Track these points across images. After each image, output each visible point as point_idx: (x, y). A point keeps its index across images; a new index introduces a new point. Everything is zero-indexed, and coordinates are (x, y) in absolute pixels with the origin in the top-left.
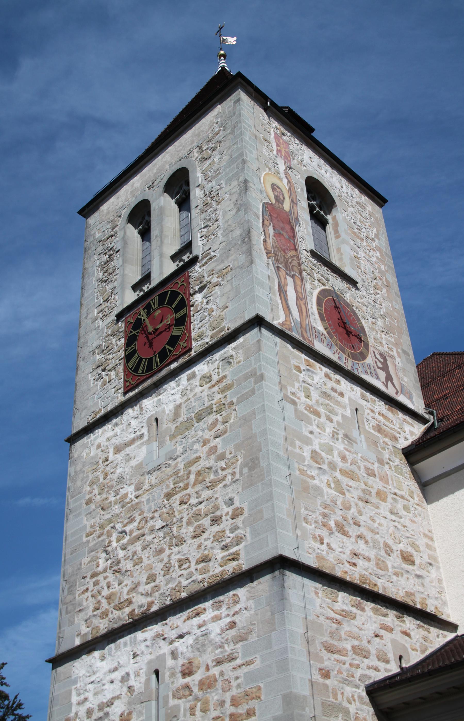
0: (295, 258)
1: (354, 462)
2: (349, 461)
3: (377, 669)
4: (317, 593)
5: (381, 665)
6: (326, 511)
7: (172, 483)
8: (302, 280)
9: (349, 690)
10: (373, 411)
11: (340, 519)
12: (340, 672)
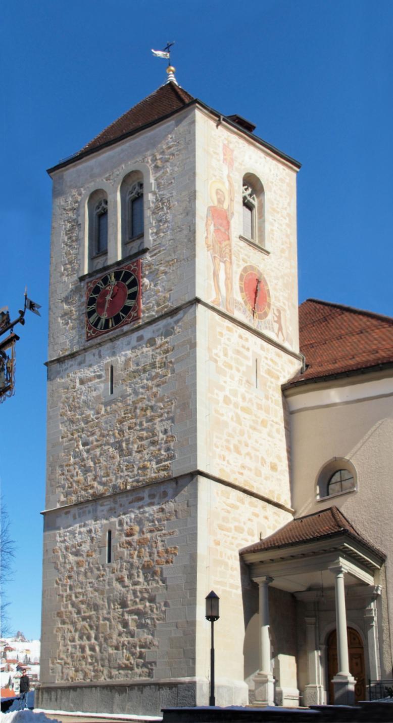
3: (247, 541)
5: (249, 538)
7: (123, 413)
8: (231, 263)
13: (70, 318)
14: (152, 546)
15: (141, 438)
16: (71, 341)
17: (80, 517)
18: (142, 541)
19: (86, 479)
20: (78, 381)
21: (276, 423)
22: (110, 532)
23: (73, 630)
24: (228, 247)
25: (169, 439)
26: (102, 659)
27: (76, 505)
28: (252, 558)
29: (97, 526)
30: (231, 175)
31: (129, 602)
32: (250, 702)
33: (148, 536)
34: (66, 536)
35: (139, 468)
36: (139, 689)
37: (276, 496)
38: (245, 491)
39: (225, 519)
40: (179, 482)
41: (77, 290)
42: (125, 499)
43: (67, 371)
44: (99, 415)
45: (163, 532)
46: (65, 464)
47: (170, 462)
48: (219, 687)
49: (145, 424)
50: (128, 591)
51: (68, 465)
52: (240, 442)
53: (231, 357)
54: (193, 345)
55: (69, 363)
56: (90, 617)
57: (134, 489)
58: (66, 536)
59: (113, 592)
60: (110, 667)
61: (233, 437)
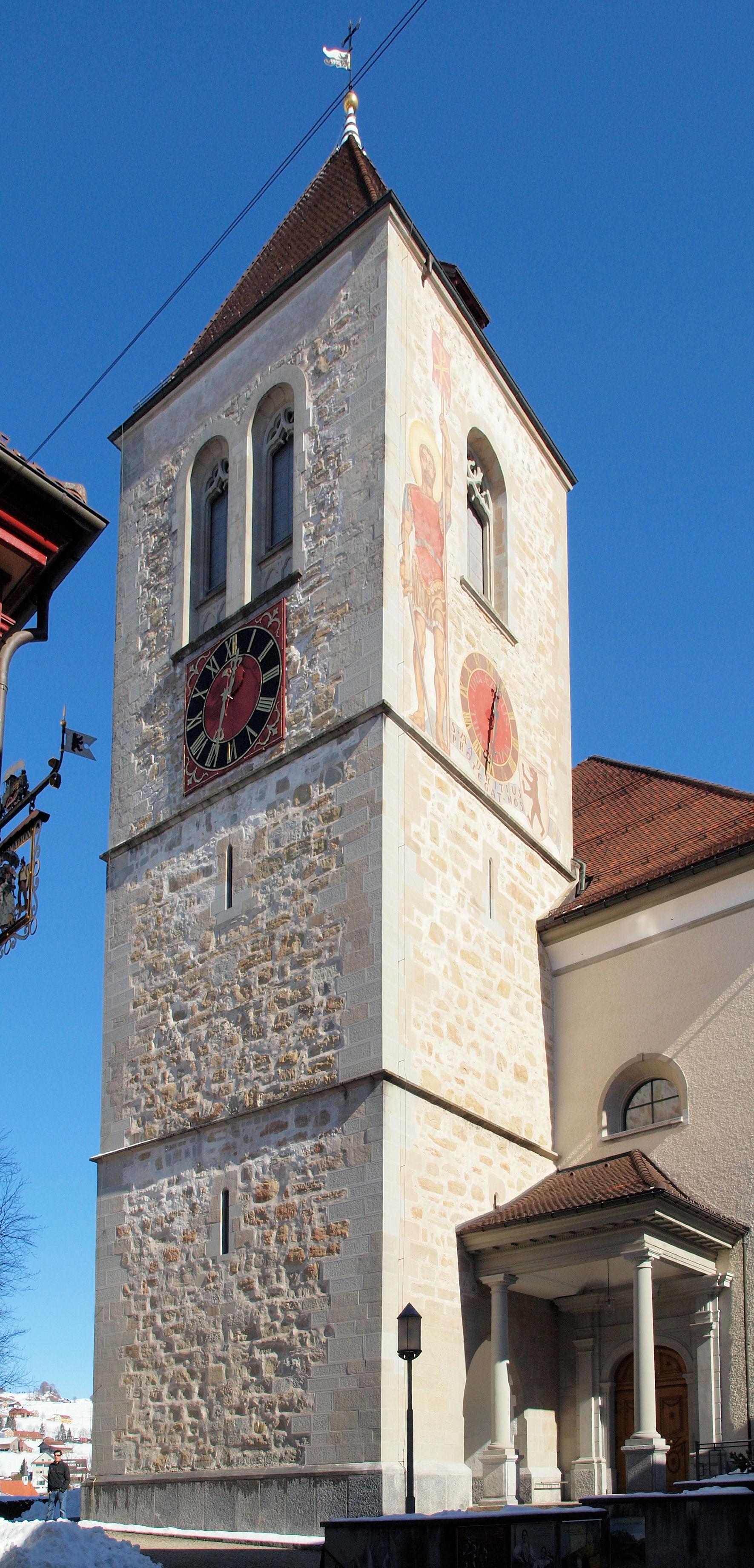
0: (439, 596)
1: (479, 940)
2: (473, 938)
4: (418, 1118)
5: (475, 1203)
6: (439, 1010)
9: (439, 1231)
10: (509, 862)
11: (453, 1021)
12: (433, 1211)
13: (154, 751)
14: (302, 1221)
15: (282, 1002)
16: (155, 800)
17: (169, 1163)
18: (284, 1210)
19: (180, 1087)
20: (166, 884)
21: (527, 992)
22: (226, 1194)
23: (157, 1380)
24: (439, 596)
25: (333, 1004)
26: (213, 1431)
27: (161, 1140)
28: (480, 1241)
29: (202, 1181)
30: (446, 418)
31: (262, 1329)
32: (476, 1500)
33: (296, 1199)
34: (142, 1202)
35: (279, 1064)
36: (279, 1484)
37: (523, 1128)
38: (468, 1116)
39: (432, 1169)
40: (347, 1095)
41: (167, 687)
42: (253, 1126)
43: (147, 865)
44: (206, 954)
45: (323, 1192)
46: (139, 1058)
47: (333, 1051)
48: (421, 1479)
49: (289, 973)
50: (260, 1308)
51: (146, 1061)
52: (459, 1019)
53: (445, 846)
54: (377, 809)
55: (151, 846)
56: (190, 1357)
57: (271, 1107)
58: (143, 1202)
59: (232, 1311)
60: (227, 1445)
61: (447, 1010)
